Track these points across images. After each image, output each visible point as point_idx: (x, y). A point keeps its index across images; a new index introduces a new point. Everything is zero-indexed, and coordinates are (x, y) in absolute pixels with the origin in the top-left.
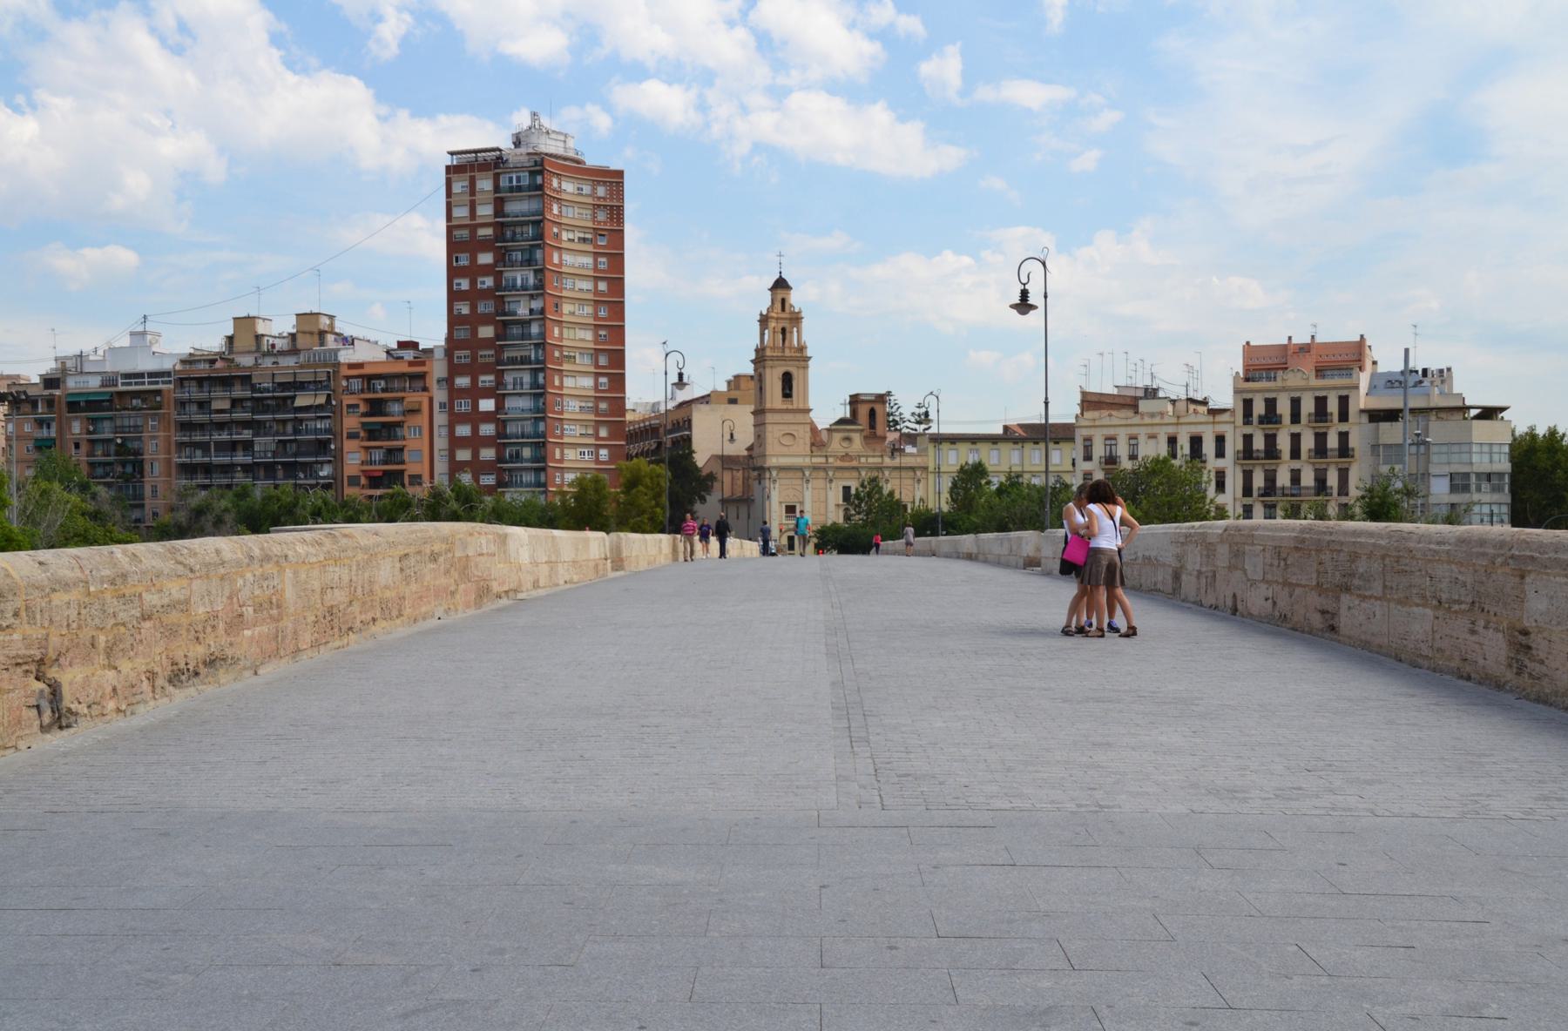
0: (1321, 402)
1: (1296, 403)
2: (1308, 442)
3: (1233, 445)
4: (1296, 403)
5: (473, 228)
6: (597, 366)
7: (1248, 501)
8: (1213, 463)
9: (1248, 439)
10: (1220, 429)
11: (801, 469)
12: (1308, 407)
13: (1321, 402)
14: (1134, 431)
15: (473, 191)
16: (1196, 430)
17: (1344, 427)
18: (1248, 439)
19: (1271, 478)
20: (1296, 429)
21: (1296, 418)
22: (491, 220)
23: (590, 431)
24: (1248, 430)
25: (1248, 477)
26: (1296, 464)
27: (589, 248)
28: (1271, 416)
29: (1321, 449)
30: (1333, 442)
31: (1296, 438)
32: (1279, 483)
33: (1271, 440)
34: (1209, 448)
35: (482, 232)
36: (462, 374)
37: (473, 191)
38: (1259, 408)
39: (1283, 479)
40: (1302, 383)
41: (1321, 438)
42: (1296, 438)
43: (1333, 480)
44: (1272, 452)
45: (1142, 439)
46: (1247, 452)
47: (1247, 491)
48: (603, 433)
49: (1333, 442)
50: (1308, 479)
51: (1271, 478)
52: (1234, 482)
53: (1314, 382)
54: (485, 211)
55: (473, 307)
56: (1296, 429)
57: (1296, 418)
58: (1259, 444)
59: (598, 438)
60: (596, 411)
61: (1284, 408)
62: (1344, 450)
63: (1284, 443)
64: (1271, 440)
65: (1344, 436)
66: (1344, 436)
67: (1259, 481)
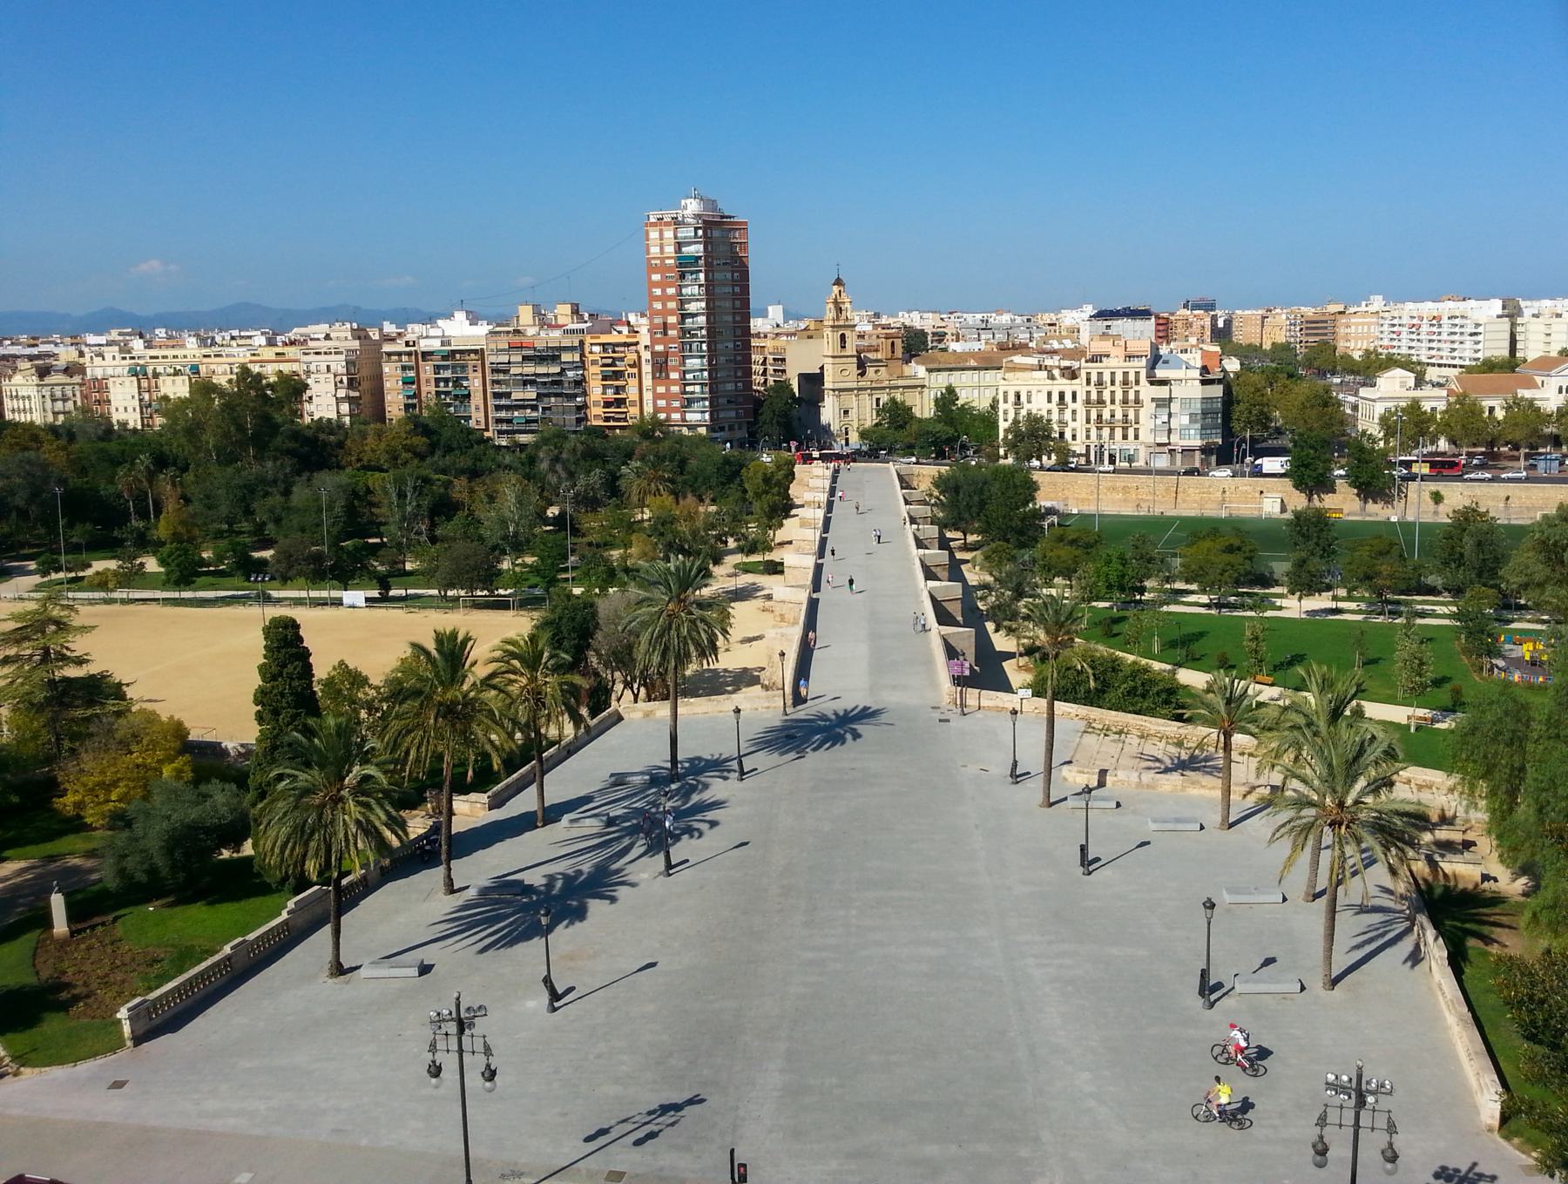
0: (1126, 374)
1: (1113, 374)
2: (1119, 396)
3: (1081, 397)
4: (1113, 374)
5: (663, 259)
6: (735, 336)
7: (1088, 426)
8: (1071, 406)
9: (1088, 393)
10: (1075, 388)
11: (852, 390)
12: (1119, 378)
13: (1126, 374)
14: (1030, 388)
15: (661, 238)
16: (1062, 388)
17: (1136, 388)
18: (1088, 393)
19: (1100, 416)
20: (1113, 388)
21: (1113, 383)
22: (674, 255)
23: (732, 373)
24: (1088, 388)
25: (1088, 412)
26: (1113, 407)
27: (730, 268)
28: (1100, 383)
29: (1125, 401)
30: (1131, 396)
31: (1113, 393)
32: (1104, 418)
33: (1100, 393)
34: (1068, 398)
35: (667, 261)
36: (658, 344)
37: (661, 238)
38: (1094, 378)
39: (1106, 415)
40: (1116, 365)
41: (1125, 393)
42: (1113, 393)
43: (1131, 416)
44: (1101, 402)
45: (1034, 393)
46: (1088, 402)
47: (1088, 421)
48: (739, 374)
49: (1131, 396)
50: (1119, 416)
51: (1100, 416)
52: (1081, 416)
53: (1123, 364)
54: (670, 250)
55: (664, 305)
56: (1113, 388)
57: (1113, 383)
58: (1094, 396)
59: (736, 377)
60: (736, 362)
61: (1107, 378)
62: (1137, 401)
63: (1106, 396)
64: (1100, 393)
65: (1137, 392)
66: (1137, 392)
67: (1094, 416)
